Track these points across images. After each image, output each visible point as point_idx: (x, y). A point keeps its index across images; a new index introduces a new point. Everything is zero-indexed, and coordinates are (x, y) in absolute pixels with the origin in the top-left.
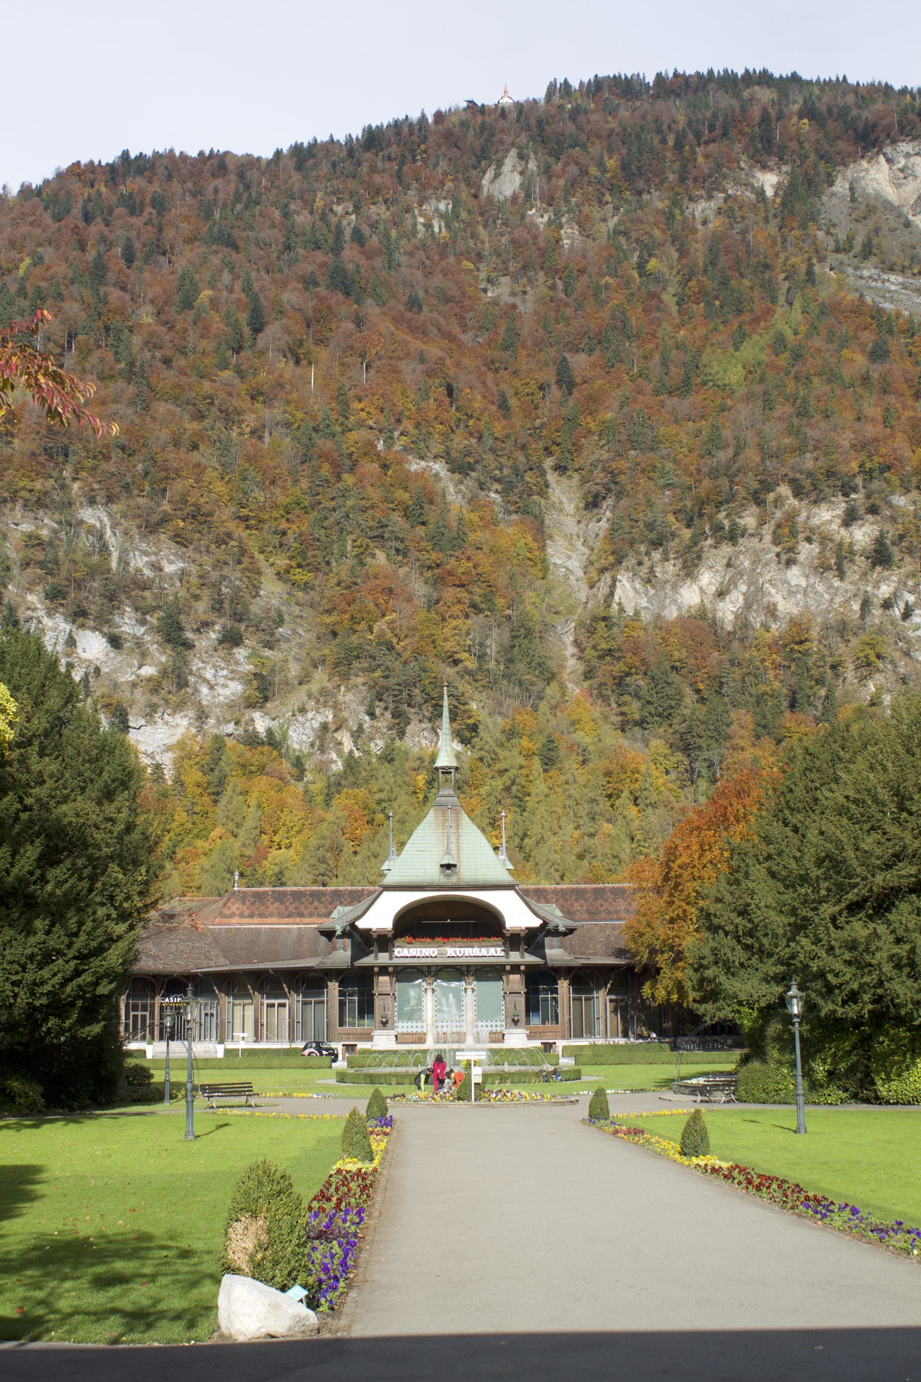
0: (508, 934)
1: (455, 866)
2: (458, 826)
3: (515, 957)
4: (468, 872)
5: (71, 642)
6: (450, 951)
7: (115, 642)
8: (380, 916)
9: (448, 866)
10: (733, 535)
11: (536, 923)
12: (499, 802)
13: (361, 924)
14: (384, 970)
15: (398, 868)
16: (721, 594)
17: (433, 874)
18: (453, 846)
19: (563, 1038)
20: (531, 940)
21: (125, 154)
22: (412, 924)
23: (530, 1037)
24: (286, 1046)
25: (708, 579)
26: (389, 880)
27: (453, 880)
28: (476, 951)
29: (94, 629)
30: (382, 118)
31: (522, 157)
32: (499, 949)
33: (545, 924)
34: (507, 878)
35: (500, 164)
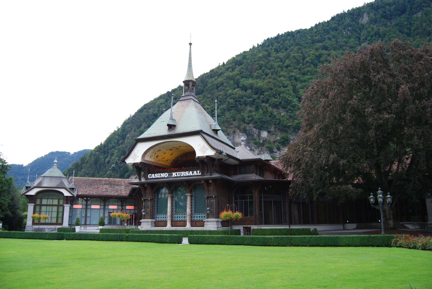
0: (198, 161)
1: (175, 126)
3: (207, 176)
4: (180, 129)
5: (259, 133)
6: (174, 174)
7: (269, 132)
11: (211, 153)
17: (164, 131)
19: (255, 224)
21: (279, 34)
27: (172, 133)
28: (187, 173)
29: (265, 130)
30: (334, 14)
31: (368, 13)
32: (198, 171)
35: (363, 16)
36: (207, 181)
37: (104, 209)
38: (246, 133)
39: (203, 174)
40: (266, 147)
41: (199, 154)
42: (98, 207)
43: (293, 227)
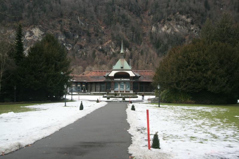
2: (124, 61)
3: (131, 81)
4: (125, 68)
6: (122, 79)
8: (112, 74)
9: (122, 67)
10: (170, 20)
11: (134, 75)
12: (130, 59)
13: (109, 75)
14: (112, 82)
15: (115, 67)
16: (168, 29)
17: (120, 68)
18: (123, 63)
19: (138, 92)
20: (133, 78)
22: (116, 76)
23: (133, 92)
24: (99, 93)
25: (166, 27)
26: (113, 69)
27: (123, 69)
28: (126, 79)
33: (136, 76)
34: (130, 69)
36: (131, 82)
37: (76, 86)
38: (65, 35)
39: (130, 80)
40: (78, 44)
41: (131, 75)
42: (74, 85)
43: (145, 93)
